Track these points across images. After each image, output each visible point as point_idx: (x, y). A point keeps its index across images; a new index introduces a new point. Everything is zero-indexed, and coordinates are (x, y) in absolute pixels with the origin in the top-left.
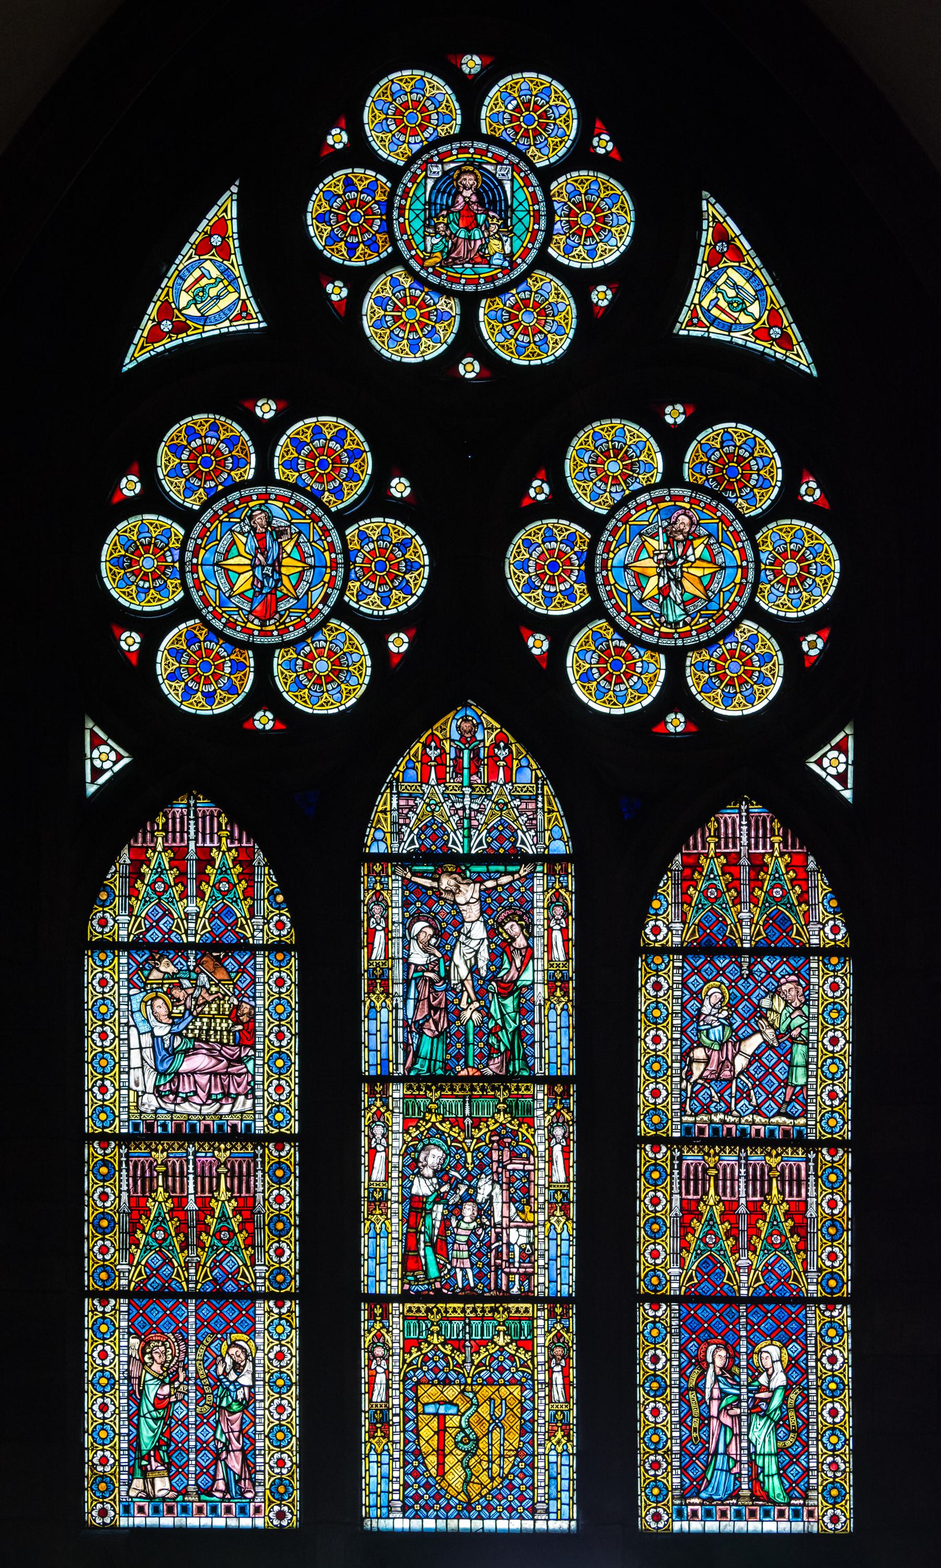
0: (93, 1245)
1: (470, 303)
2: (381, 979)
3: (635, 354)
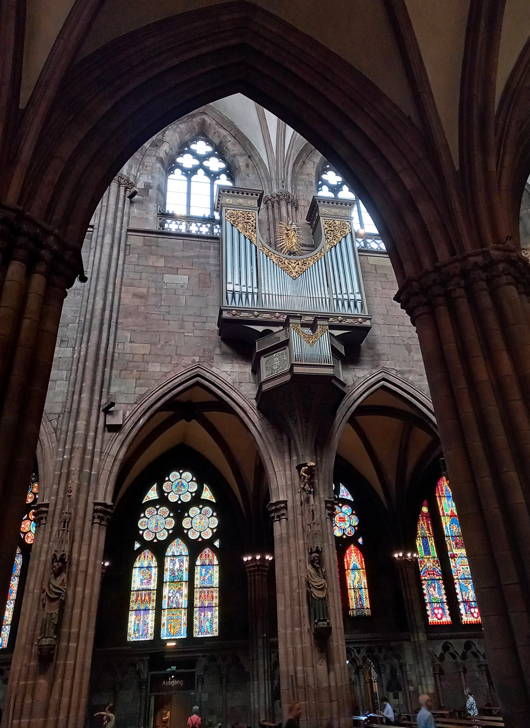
0: (131, 604)
1: (180, 495)
2: (167, 570)
3: (196, 500)
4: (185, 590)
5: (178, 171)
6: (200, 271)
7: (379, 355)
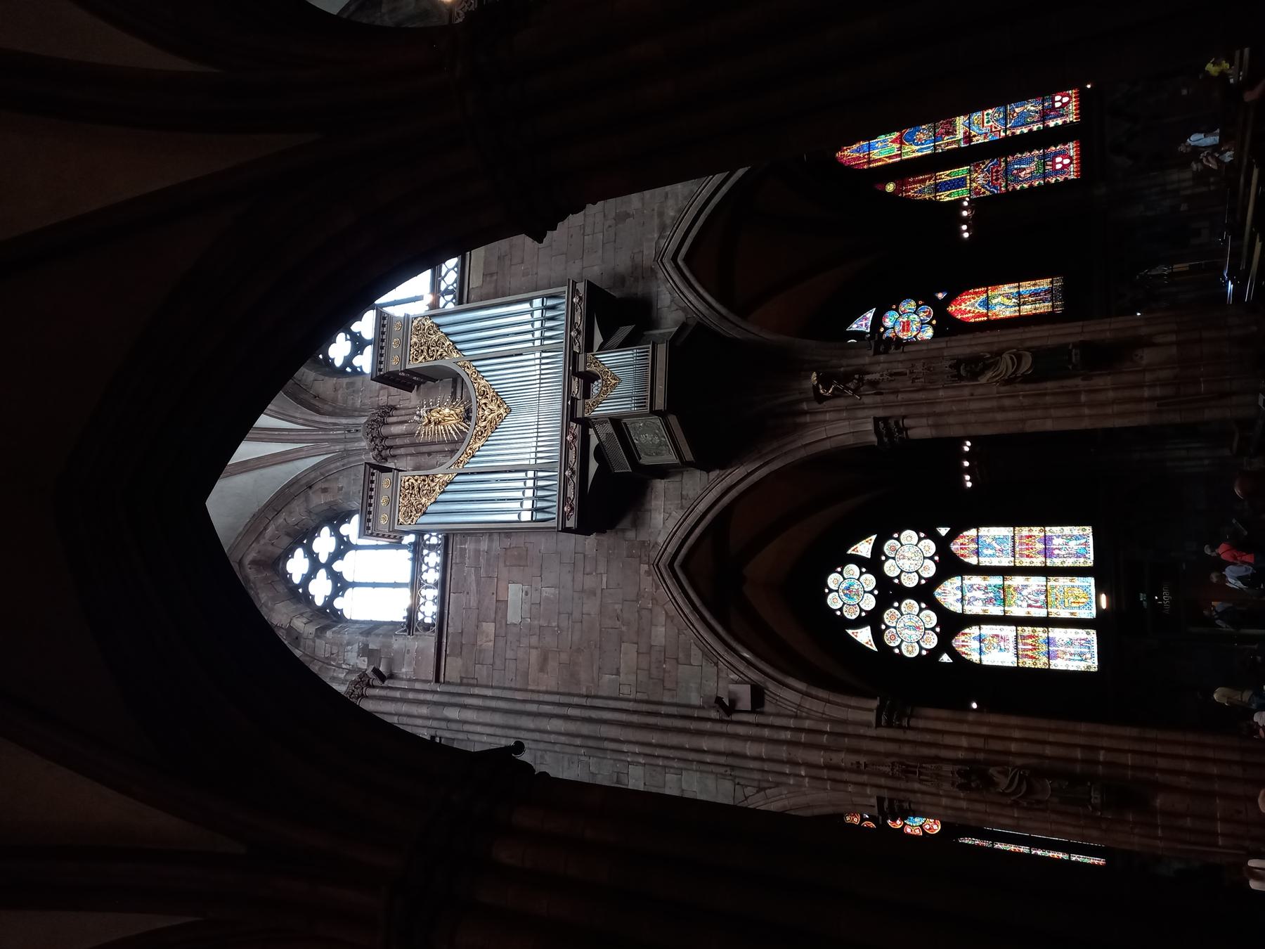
0: (1039, 666)
3: (873, 564)
4: (1017, 581)
5: (338, 603)
6: (501, 565)
7: (635, 267)
